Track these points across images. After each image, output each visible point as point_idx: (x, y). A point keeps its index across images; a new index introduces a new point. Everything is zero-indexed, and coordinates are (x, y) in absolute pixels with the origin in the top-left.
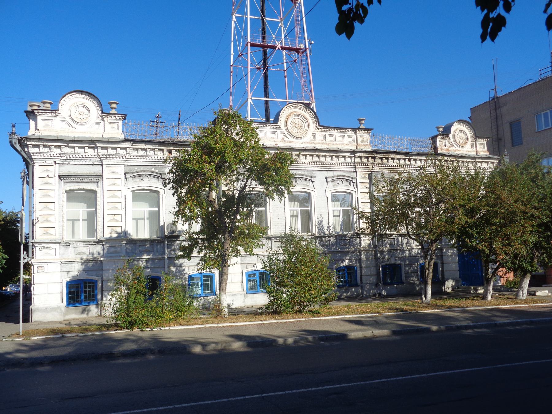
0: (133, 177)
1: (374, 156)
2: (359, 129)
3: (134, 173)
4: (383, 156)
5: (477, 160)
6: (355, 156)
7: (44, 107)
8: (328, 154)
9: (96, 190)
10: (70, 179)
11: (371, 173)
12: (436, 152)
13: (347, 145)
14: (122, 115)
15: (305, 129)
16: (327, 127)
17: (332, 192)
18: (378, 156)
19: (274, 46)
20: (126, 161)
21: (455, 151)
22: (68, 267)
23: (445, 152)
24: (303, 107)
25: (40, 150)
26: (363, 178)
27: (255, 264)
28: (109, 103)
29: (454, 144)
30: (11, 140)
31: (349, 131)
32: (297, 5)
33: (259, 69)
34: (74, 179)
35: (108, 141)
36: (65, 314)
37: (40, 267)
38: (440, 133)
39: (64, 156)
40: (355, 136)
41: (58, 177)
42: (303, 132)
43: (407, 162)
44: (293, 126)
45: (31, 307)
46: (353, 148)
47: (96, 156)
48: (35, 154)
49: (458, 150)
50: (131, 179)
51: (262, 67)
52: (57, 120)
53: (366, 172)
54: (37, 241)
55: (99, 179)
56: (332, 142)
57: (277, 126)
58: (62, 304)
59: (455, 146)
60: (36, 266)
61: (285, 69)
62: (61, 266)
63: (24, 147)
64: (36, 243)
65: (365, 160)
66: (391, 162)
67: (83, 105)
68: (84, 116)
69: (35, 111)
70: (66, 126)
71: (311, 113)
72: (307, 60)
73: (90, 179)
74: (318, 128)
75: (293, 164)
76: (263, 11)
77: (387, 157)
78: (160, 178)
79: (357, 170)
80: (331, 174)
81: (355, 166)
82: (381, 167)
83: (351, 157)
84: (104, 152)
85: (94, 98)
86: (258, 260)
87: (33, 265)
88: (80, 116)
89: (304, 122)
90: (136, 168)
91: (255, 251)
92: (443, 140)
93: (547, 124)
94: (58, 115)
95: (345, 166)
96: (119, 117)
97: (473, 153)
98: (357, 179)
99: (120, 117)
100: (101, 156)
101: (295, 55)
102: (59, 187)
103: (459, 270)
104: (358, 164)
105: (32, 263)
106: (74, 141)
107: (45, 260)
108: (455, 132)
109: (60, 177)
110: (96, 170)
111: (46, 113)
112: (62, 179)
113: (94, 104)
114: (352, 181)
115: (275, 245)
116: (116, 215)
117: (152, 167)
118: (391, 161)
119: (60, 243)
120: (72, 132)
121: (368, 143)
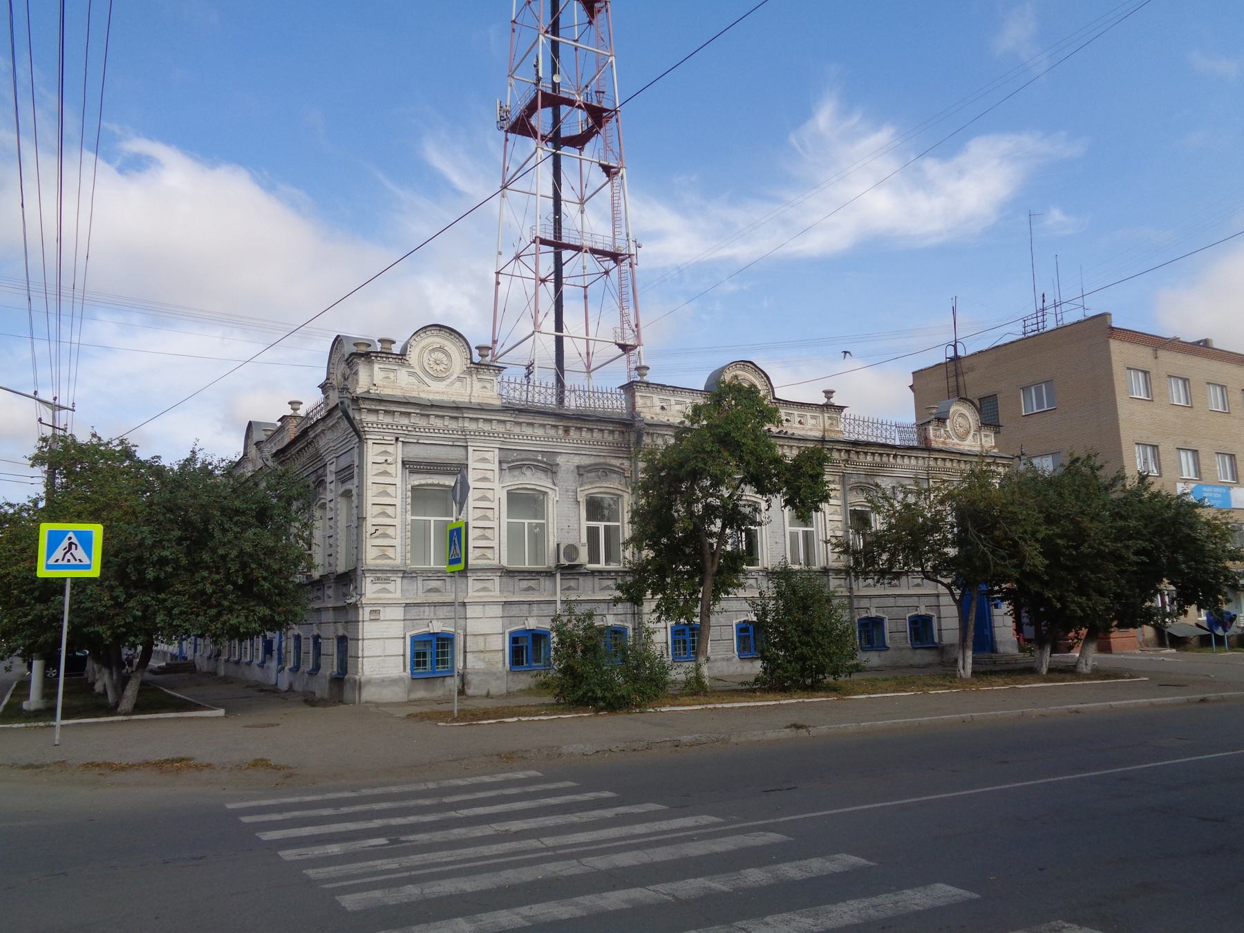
0: (510, 468)
3: (513, 461)
12: (929, 445)
13: (811, 430)
22: (414, 612)
36: (410, 692)
43: (891, 459)
47: (460, 433)
48: (370, 425)
51: (552, 277)
60: (367, 610)
68: (441, 367)
70: (413, 380)
78: (549, 472)
84: (471, 426)
88: (435, 367)
93: (1040, 405)
97: (977, 449)
101: (612, 264)
106: (433, 406)
107: (380, 599)
109: (403, 463)
110: (454, 455)
116: (487, 530)
118: (869, 458)
119: (404, 572)
120: (424, 391)
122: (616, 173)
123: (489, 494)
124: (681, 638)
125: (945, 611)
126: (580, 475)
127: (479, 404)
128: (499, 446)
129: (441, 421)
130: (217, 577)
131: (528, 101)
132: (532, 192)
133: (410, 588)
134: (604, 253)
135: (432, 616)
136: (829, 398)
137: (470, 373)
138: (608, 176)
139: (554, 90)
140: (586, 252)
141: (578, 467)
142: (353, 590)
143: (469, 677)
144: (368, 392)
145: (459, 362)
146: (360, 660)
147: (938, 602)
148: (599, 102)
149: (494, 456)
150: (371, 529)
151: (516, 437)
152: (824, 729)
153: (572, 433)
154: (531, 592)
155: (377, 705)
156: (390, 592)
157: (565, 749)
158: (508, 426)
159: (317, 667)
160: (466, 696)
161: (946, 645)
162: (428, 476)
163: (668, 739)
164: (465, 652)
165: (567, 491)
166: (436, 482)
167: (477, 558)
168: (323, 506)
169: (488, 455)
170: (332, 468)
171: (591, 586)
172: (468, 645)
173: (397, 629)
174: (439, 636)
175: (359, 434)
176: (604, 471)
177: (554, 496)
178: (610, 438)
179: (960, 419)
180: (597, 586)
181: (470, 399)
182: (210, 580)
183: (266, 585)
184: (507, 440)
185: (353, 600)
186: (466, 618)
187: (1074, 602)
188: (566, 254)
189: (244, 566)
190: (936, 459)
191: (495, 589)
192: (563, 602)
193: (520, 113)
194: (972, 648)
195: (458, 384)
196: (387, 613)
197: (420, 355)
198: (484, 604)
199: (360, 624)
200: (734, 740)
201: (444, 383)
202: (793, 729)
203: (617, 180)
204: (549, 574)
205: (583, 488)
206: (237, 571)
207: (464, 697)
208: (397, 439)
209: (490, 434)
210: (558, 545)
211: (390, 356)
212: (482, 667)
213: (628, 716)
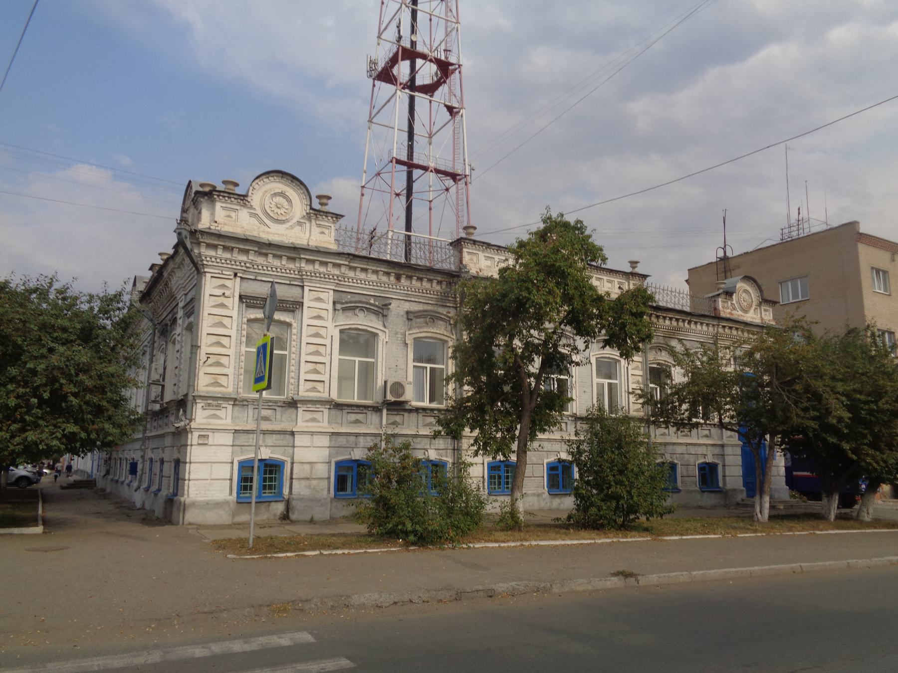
0: (344, 309)
3: (347, 303)
10: (255, 302)
17: (597, 356)
18: (655, 313)
21: (739, 316)
22: (243, 439)
25: (218, 253)
36: (234, 515)
37: (202, 435)
39: (251, 266)
40: (627, 284)
41: (238, 296)
43: (686, 324)
47: (296, 273)
48: (208, 259)
49: (741, 315)
50: (341, 311)
51: (405, 192)
52: (244, 214)
55: (298, 307)
58: (231, 497)
60: (196, 434)
62: (233, 436)
67: (282, 194)
69: (214, 193)
70: (254, 221)
73: (284, 305)
77: (665, 315)
78: (381, 315)
84: (309, 268)
87: (192, 432)
88: (276, 210)
92: (725, 300)
93: (795, 295)
94: (247, 203)
96: (332, 217)
99: (334, 219)
100: (304, 273)
101: (451, 182)
103: (786, 477)
105: (191, 428)
106: (270, 245)
107: (210, 424)
112: (244, 301)
113: (299, 195)
116: (318, 365)
117: (370, 297)
118: (667, 322)
119: (235, 400)
120: (264, 232)
122: (458, 113)
123: (322, 332)
124: (496, 473)
125: (729, 460)
126: (408, 319)
127: (316, 247)
128: (334, 288)
129: (279, 261)
130: (21, 390)
131: (391, 55)
132: (391, 126)
133: (240, 415)
134: (446, 173)
136: (634, 268)
137: (309, 219)
138: (451, 115)
139: (412, 46)
140: (431, 171)
141: (408, 313)
142: (182, 415)
143: (294, 503)
144: (209, 228)
145: (299, 207)
146: (186, 482)
147: (723, 451)
148: (446, 58)
149: (329, 297)
150: (203, 357)
152: (652, 579)
153: (403, 280)
154: (359, 425)
155: (199, 527)
156: (221, 418)
157: (356, 599)
158: (343, 269)
159: (159, 490)
160: (291, 521)
161: (730, 490)
163: (480, 587)
164: (292, 478)
165: (396, 334)
167: (308, 391)
168: (174, 343)
169: (322, 295)
170: (181, 304)
171: (416, 422)
172: (295, 472)
173: (225, 454)
174: (266, 462)
175: (198, 268)
176: (432, 318)
177: (384, 337)
178: (438, 288)
179: (744, 295)
180: (421, 422)
181: (308, 242)
182: (15, 394)
183: (74, 401)
184: (342, 283)
185: (182, 424)
187: (867, 455)
188: (416, 173)
189: (53, 380)
190: (724, 327)
191: (324, 420)
193: (385, 65)
195: (298, 228)
198: (312, 433)
199: (189, 447)
200: (556, 589)
201: (284, 225)
202: (622, 578)
203: (458, 118)
204: (376, 409)
205: (411, 332)
206: (45, 385)
207: (288, 521)
208: (236, 275)
210: (386, 382)
211: (232, 196)
212: (308, 493)
213: (439, 552)
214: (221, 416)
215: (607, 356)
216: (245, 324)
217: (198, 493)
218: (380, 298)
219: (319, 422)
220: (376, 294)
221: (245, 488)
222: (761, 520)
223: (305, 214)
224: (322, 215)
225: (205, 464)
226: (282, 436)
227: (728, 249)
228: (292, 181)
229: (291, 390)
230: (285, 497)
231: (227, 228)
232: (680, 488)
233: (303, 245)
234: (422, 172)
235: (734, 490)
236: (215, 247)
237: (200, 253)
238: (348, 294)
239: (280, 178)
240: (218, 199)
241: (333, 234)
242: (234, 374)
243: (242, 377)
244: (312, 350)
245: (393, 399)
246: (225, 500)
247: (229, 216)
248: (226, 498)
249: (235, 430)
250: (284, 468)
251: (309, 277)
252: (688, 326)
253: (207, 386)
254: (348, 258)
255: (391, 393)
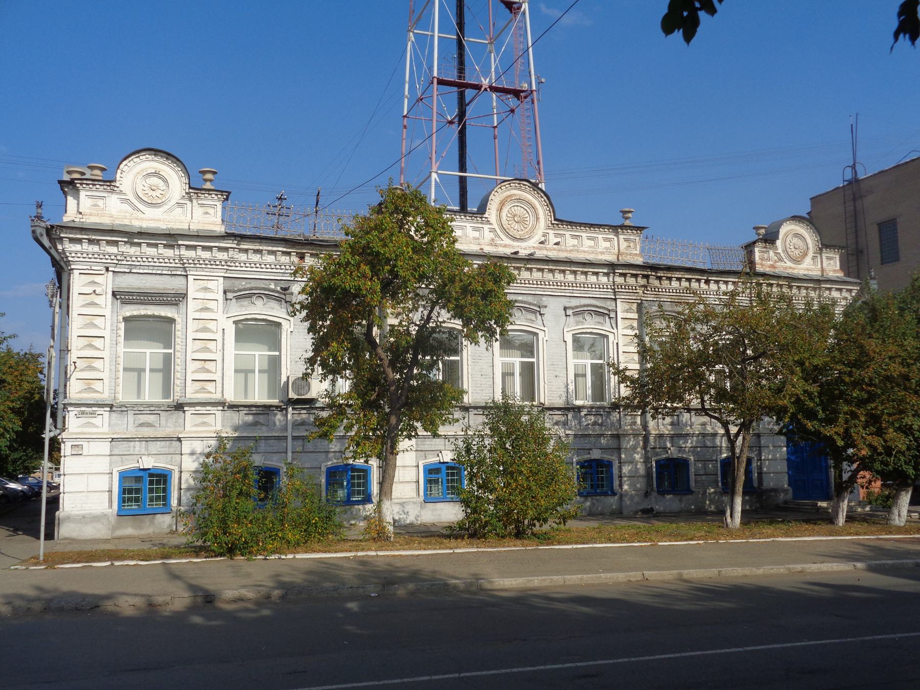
0: (238, 298)
1: (646, 273)
2: (623, 227)
3: (240, 290)
4: (662, 275)
5: (823, 286)
6: (614, 273)
7: (91, 175)
8: (569, 269)
9: (176, 317)
10: (131, 297)
11: (641, 303)
13: (602, 253)
14: (222, 192)
15: (530, 225)
16: (567, 222)
18: (653, 274)
19: (478, 85)
20: (227, 270)
21: (786, 268)
22: (122, 448)
23: (767, 269)
24: (529, 186)
25: (83, 247)
26: (627, 311)
27: (441, 452)
28: (200, 172)
29: (784, 257)
30: (33, 228)
31: (606, 230)
32: (519, 17)
33: (451, 122)
34: (138, 298)
35: (198, 236)
36: (114, 529)
38: (761, 237)
40: (616, 239)
41: (111, 293)
42: (528, 229)
43: (703, 285)
44: (510, 219)
45: (57, 513)
46: (612, 258)
47: (177, 261)
48: (73, 255)
49: (791, 268)
50: (234, 300)
51: (456, 120)
53: (633, 301)
54: (73, 402)
55: (181, 299)
56: (576, 248)
57: (483, 219)
58: (111, 510)
59: (785, 260)
61: (495, 124)
63: (56, 241)
64: (71, 405)
65: (631, 281)
66: (676, 285)
67: (156, 174)
68: (158, 193)
70: (126, 207)
71: (542, 197)
72: (533, 110)
73: (165, 299)
74: (553, 224)
75: (513, 283)
76: (461, 24)
77: (670, 275)
79: (617, 297)
80: (574, 302)
81: (614, 289)
82: (658, 293)
83: (607, 274)
84: (191, 254)
85: (177, 162)
86: (445, 445)
87: (64, 442)
88: (151, 193)
89: (530, 213)
90: (244, 283)
91: (442, 430)
92: (763, 250)
94: (116, 189)
95: (597, 290)
96: (217, 195)
97: (816, 273)
98: (616, 312)
99: (219, 196)
100: (185, 261)
101: (512, 101)
102: (112, 312)
104: (620, 287)
106: (141, 234)
108: (786, 235)
109: (114, 294)
111: (95, 185)
112: (118, 297)
113: (177, 172)
114: (609, 315)
115: (477, 421)
116: (207, 362)
117: (270, 281)
118: (675, 284)
119: (111, 406)
120: (137, 219)
121: (638, 252)
122: (519, 8)
123: (211, 325)
124: (434, 477)
133: (119, 422)
135: (143, 451)
149: (218, 285)
151: (242, 265)
156: (97, 427)
158: (231, 252)
162: (143, 307)
166: (149, 313)
167: (196, 392)
169: (210, 285)
173: (103, 464)
179: (795, 240)
186: (182, 454)
188: (469, 93)
192: (295, 438)
194: (741, 494)
195: (179, 210)
196: (89, 448)
197: (134, 183)
201: (161, 209)
208: (107, 269)
209: (213, 262)
214: (97, 424)
215: (589, 331)
216: (120, 322)
217: (73, 506)
218: (283, 282)
219: (212, 426)
220: (276, 278)
221: (130, 500)
222: (730, 526)
223: (184, 194)
224: (204, 194)
225: (80, 476)
226: (168, 442)
227: (858, 167)
228: (167, 158)
229: (177, 392)
230: (173, 509)
231: (92, 219)
232: (693, 489)
233: (182, 229)
234: (475, 92)
235: (775, 490)
236: (79, 241)
237: (63, 250)
238: (243, 280)
239: (153, 157)
240: (81, 187)
241: (219, 213)
242: (110, 378)
243: (120, 381)
244: (199, 347)
245: (296, 397)
246: (103, 513)
247: (96, 205)
248: (103, 511)
249: (113, 439)
250: (171, 478)
251: (192, 265)
252: (706, 287)
253: (80, 392)
254: (235, 240)
255: (293, 390)
